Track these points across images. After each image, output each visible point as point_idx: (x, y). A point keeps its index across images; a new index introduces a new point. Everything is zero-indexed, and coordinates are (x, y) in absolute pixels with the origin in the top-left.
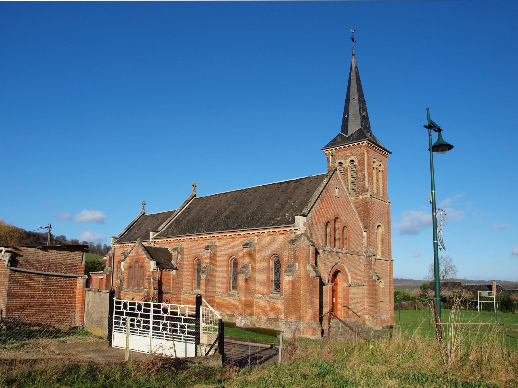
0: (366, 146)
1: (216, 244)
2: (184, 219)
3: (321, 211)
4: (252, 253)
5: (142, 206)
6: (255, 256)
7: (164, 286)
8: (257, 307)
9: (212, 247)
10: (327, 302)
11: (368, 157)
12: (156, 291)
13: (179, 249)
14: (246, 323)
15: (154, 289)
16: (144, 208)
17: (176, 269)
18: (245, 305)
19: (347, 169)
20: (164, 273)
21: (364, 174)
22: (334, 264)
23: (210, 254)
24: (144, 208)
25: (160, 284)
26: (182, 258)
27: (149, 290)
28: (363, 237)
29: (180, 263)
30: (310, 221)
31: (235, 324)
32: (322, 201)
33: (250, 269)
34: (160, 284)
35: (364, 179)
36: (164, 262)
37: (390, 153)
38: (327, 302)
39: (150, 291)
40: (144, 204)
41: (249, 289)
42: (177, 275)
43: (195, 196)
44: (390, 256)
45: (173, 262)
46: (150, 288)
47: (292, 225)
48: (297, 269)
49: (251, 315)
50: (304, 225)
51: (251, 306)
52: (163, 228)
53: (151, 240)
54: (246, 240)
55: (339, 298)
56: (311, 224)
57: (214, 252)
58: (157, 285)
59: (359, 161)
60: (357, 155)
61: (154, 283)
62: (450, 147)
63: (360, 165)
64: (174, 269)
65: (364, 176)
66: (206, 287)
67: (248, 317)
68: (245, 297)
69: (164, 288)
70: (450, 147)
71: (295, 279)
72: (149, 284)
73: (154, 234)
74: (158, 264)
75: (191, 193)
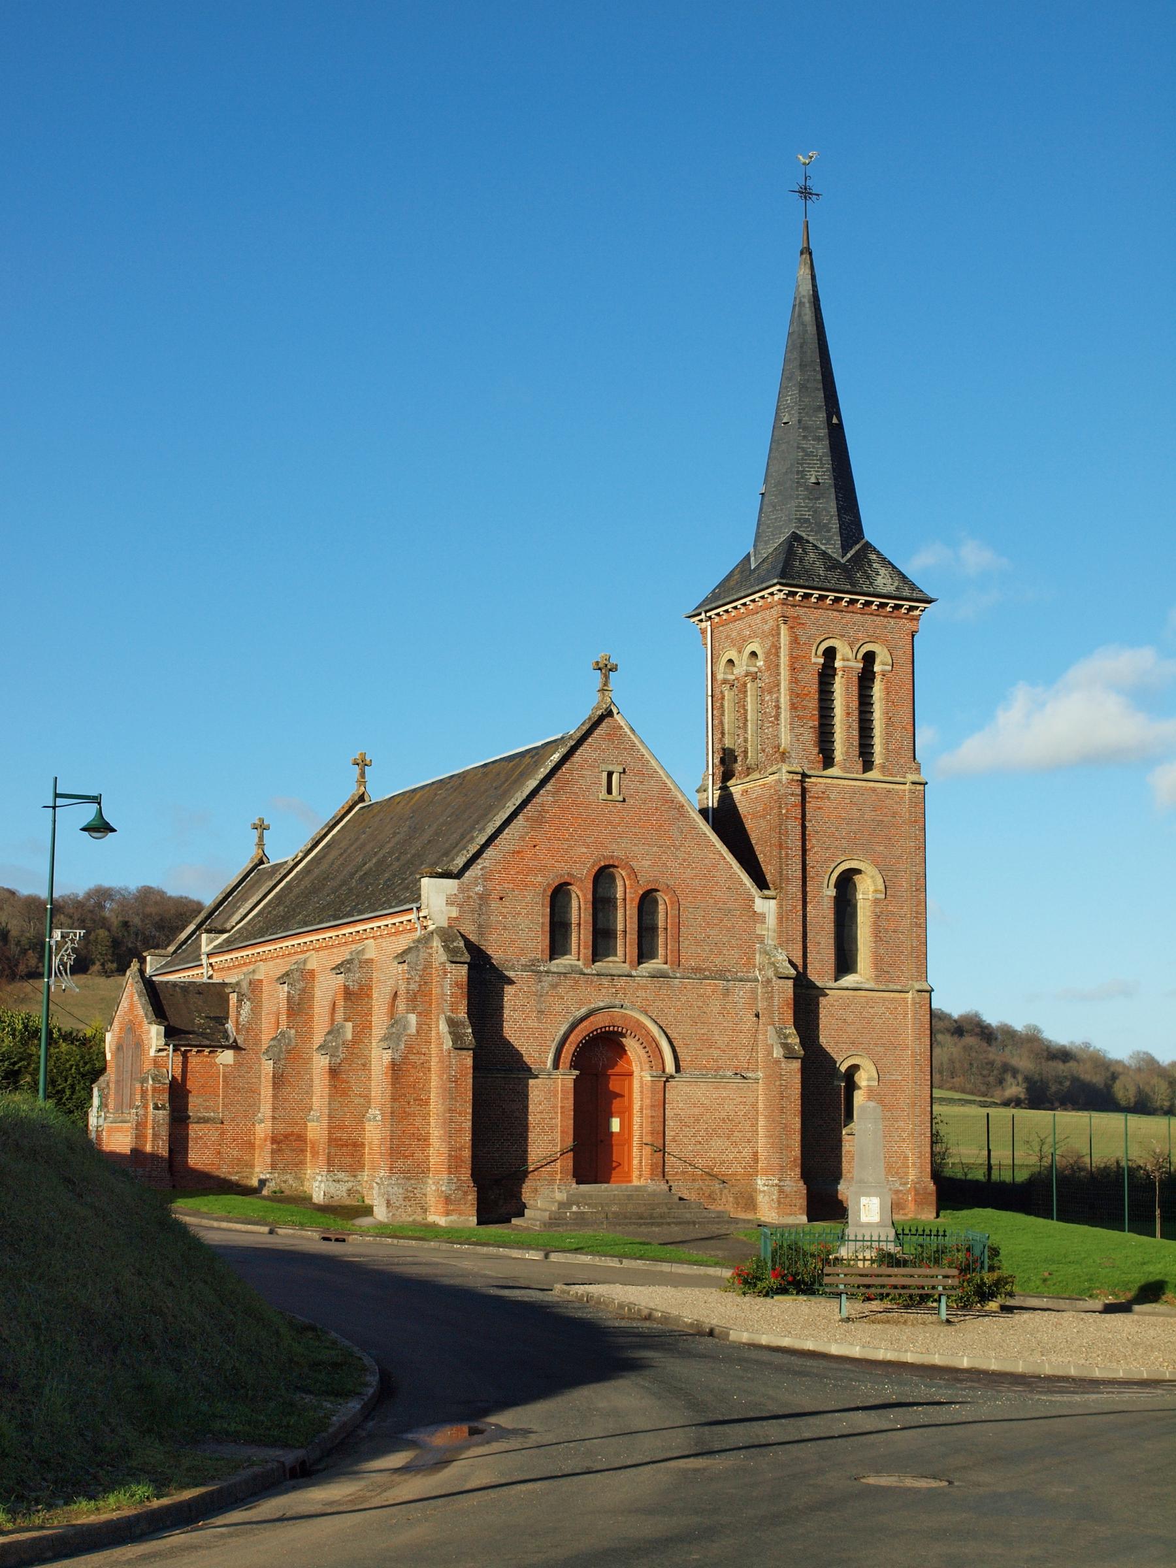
0: (784, 602)
1: (309, 966)
2: (298, 885)
3: (529, 854)
4: (354, 988)
5: (256, 833)
6: (369, 996)
7: (193, 1101)
8: (370, 1143)
9: (296, 975)
10: (552, 1128)
11: (795, 640)
12: (163, 1114)
13: (245, 985)
14: (332, 1190)
15: (156, 1108)
16: (261, 843)
17: (235, 1047)
18: (330, 1140)
19: (745, 685)
20: (194, 1060)
21: (778, 701)
22: (583, 1011)
23: (289, 998)
24: (261, 843)
25: (178, 1093)
26: (256, 1011)
27: (141, 1112)
28: (761, 918)
29: (250, 1029)
30: (479, 889)
31: (311, 1198)
32: (538, 822)
33: (349, 1036)
34: (178, 1093)
35: (777, 717)
36: (200, 1025)
37: (929, 601)
38: (552, 1128)
39: (146, 1116)
40: (261, 827)
41: (345, 1094)
42: (238, 1064)
43: (362, 798)
44: (923, 974)
45: (230, 1026)
46: (145, 1107)
47: (414, 906)
48: (413, 1030)
49: (355, 1167)
50: (449, 903)
51: (355, 1145)
52: (237, 920)
53: (204, 957)
54: (343, 954)
55: (636, 1120)
56: (483, 898)
57: (303, 990)
58: (166, 1096)
59: (767, 654)
60: (764, 636)
61: (154, 1090)
62: (83, 829)
63: (768, 668)
64: (228, 1047)
65: (778, 707)
66: (275, 1096)
67: (341, 1175)
68: (330, 1117)
69: (196, 1105)
70: (83, 829)
71: (406, 1057)
72: (144, 1093)
73: (212, 942)
74: (171, 1033)
75: (352, 791)
